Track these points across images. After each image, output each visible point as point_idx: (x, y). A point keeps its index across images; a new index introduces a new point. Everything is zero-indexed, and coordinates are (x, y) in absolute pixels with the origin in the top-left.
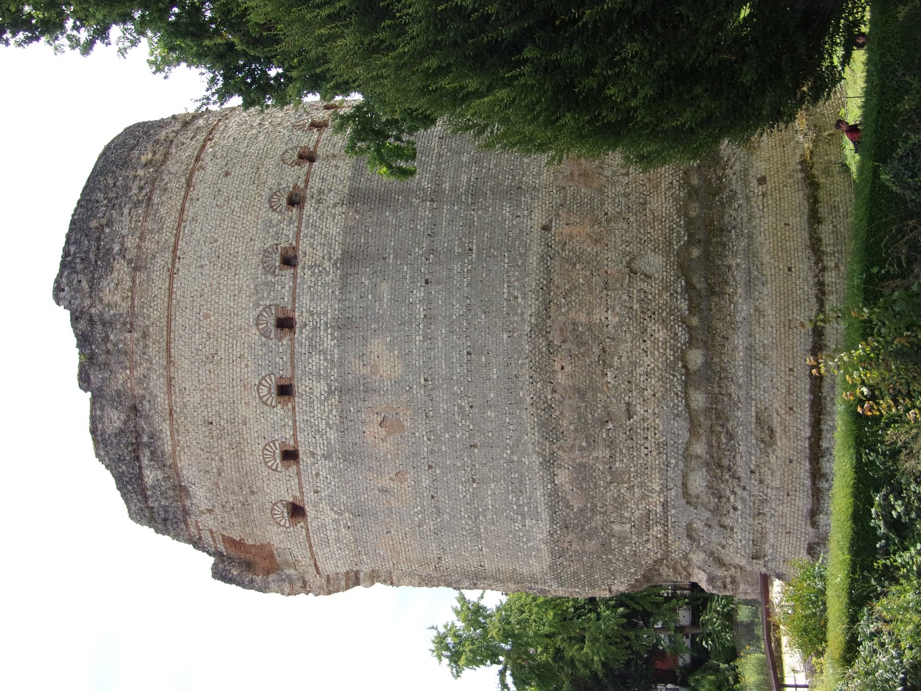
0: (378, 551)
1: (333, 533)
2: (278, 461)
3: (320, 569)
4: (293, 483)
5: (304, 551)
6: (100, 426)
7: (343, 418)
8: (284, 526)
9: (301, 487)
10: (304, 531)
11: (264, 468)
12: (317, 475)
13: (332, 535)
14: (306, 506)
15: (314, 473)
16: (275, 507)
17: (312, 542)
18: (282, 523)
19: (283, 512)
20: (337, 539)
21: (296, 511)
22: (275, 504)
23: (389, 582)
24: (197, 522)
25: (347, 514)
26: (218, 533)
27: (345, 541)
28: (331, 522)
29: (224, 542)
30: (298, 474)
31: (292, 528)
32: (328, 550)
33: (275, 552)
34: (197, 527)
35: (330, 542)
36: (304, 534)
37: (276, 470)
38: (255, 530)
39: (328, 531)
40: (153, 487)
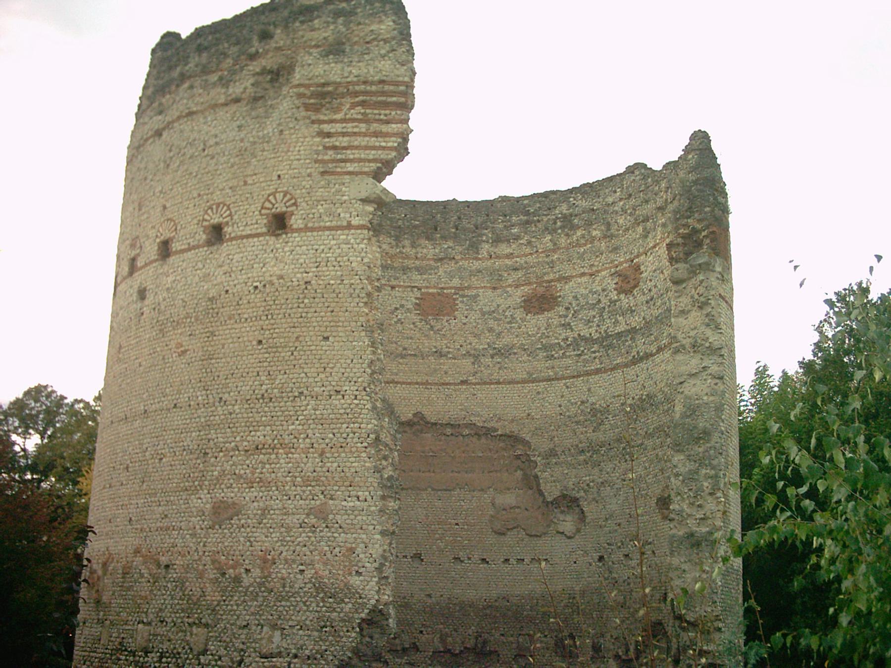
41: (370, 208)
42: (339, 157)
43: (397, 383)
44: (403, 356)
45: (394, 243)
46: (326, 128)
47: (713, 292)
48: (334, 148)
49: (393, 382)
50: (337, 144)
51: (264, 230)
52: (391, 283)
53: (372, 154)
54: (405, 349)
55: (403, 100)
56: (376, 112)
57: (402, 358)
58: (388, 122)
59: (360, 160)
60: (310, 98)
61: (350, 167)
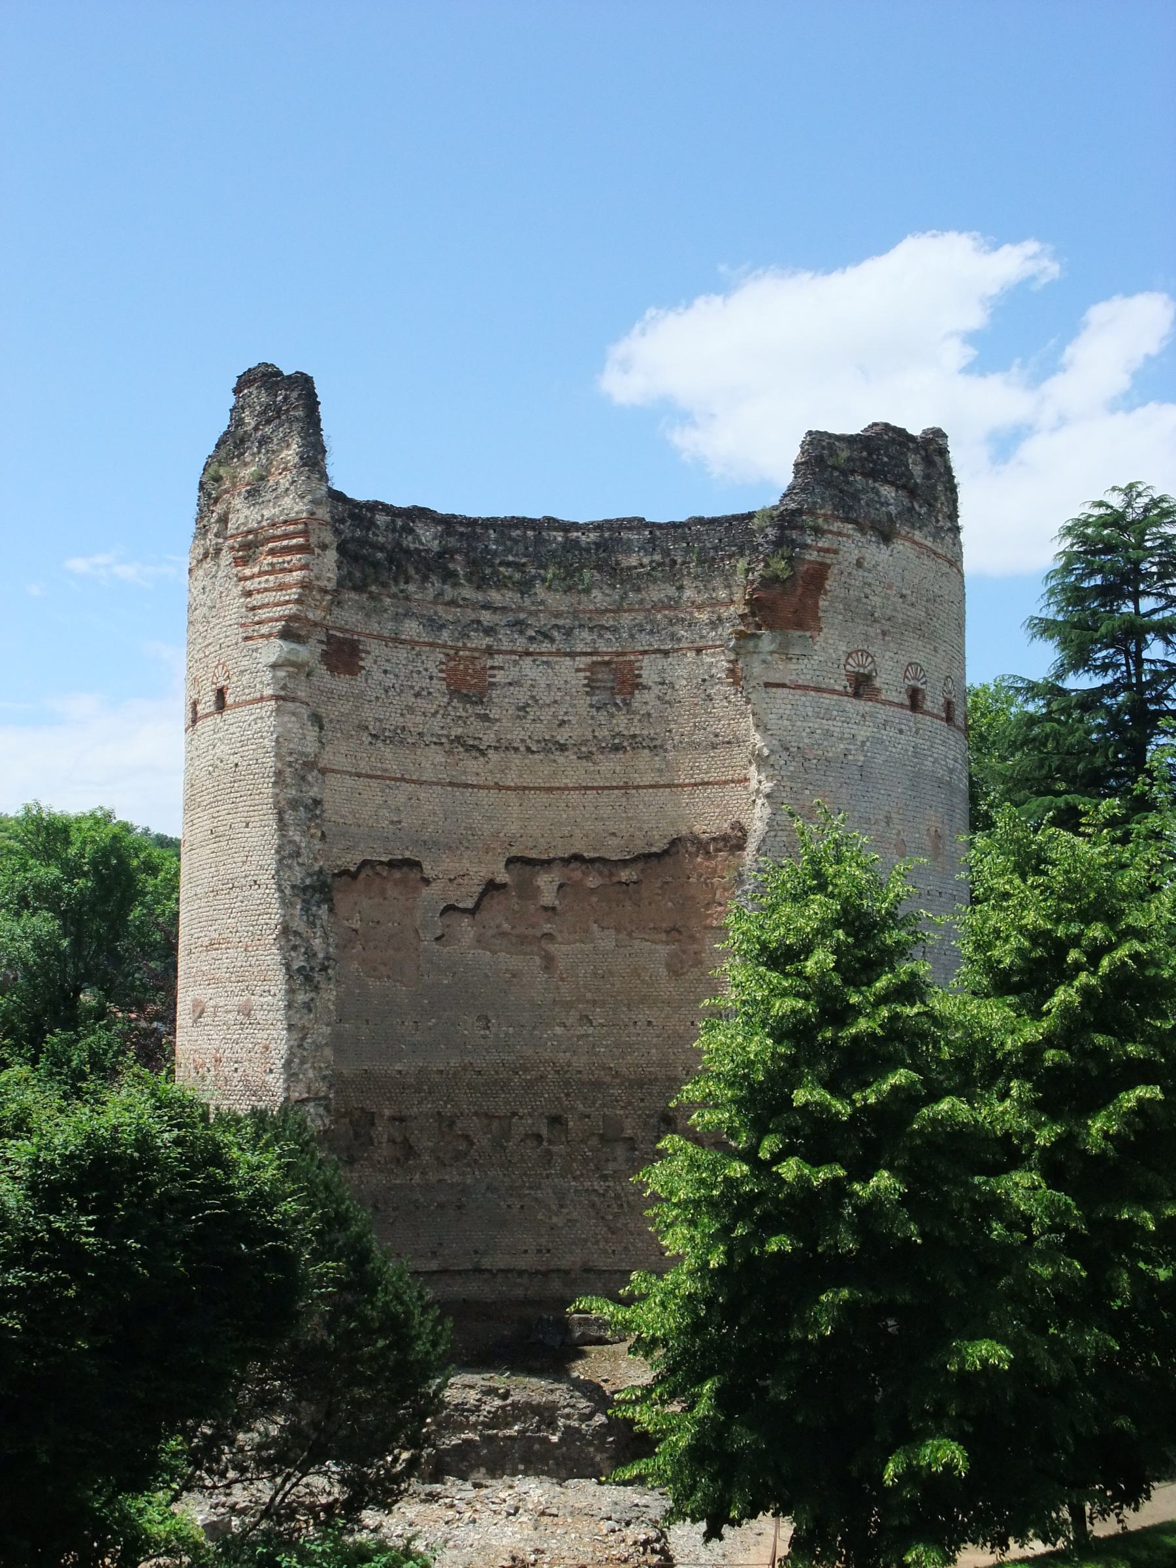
0: (810, 787)
1: (838, 729)
2: (912, 683)
3: (774, 690)
4: (894, 694)
5: (809, 677)
6: (911, 445)
7: (940, 782)
8: (847, 663)
9: (891, 703)
10: (841, 688)
11: (905, 660)
12: (901, 731)
13: (836, 727)
14: (870, 703)
15: (903, 727)
16: (870, 659)
17: (825, 695)
18: (850, 661)
19: (865, 667)
20: (828, 734)
21: (861, 686)
22: (873, 661)
23: (282, 693)
24: (848, 536)
25: (862, 758)
26: (835, 561)
27: (826, 743)
28: (853, 732)
29: (821, 564)
30: (901, 705)
31: (844, 672)
32: (810, 714)
33: (808, 634)
34: (840, 534)
35: (824, 722)
36: (837, 687)
37: (906, 677)
38: (840, 617)
39: (840, 724)
40: (878, 493)
41: (281, 674)
42: (257, 618)
43: (708, 783)
44: (714, 747)
45: (701, 585)
46: (249, 585)
47: (754, 683)
48: (253, 609)
49: (704, 784)
50: (255, 603)
51: (212, 709)
52: (696, 645)
53: (279, 611)
54: (717, 736)
55: (301, 540)
56: (281, 560)
57: (714, 748)
58: (291, 571)
59: (271, 620)
60: (238, 551)
61: (265, 629)
